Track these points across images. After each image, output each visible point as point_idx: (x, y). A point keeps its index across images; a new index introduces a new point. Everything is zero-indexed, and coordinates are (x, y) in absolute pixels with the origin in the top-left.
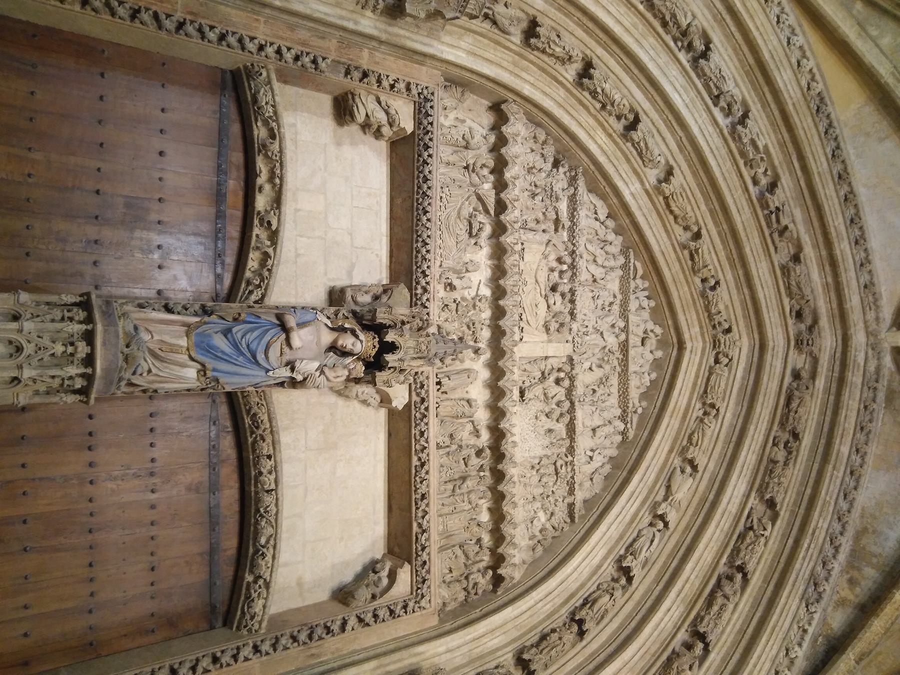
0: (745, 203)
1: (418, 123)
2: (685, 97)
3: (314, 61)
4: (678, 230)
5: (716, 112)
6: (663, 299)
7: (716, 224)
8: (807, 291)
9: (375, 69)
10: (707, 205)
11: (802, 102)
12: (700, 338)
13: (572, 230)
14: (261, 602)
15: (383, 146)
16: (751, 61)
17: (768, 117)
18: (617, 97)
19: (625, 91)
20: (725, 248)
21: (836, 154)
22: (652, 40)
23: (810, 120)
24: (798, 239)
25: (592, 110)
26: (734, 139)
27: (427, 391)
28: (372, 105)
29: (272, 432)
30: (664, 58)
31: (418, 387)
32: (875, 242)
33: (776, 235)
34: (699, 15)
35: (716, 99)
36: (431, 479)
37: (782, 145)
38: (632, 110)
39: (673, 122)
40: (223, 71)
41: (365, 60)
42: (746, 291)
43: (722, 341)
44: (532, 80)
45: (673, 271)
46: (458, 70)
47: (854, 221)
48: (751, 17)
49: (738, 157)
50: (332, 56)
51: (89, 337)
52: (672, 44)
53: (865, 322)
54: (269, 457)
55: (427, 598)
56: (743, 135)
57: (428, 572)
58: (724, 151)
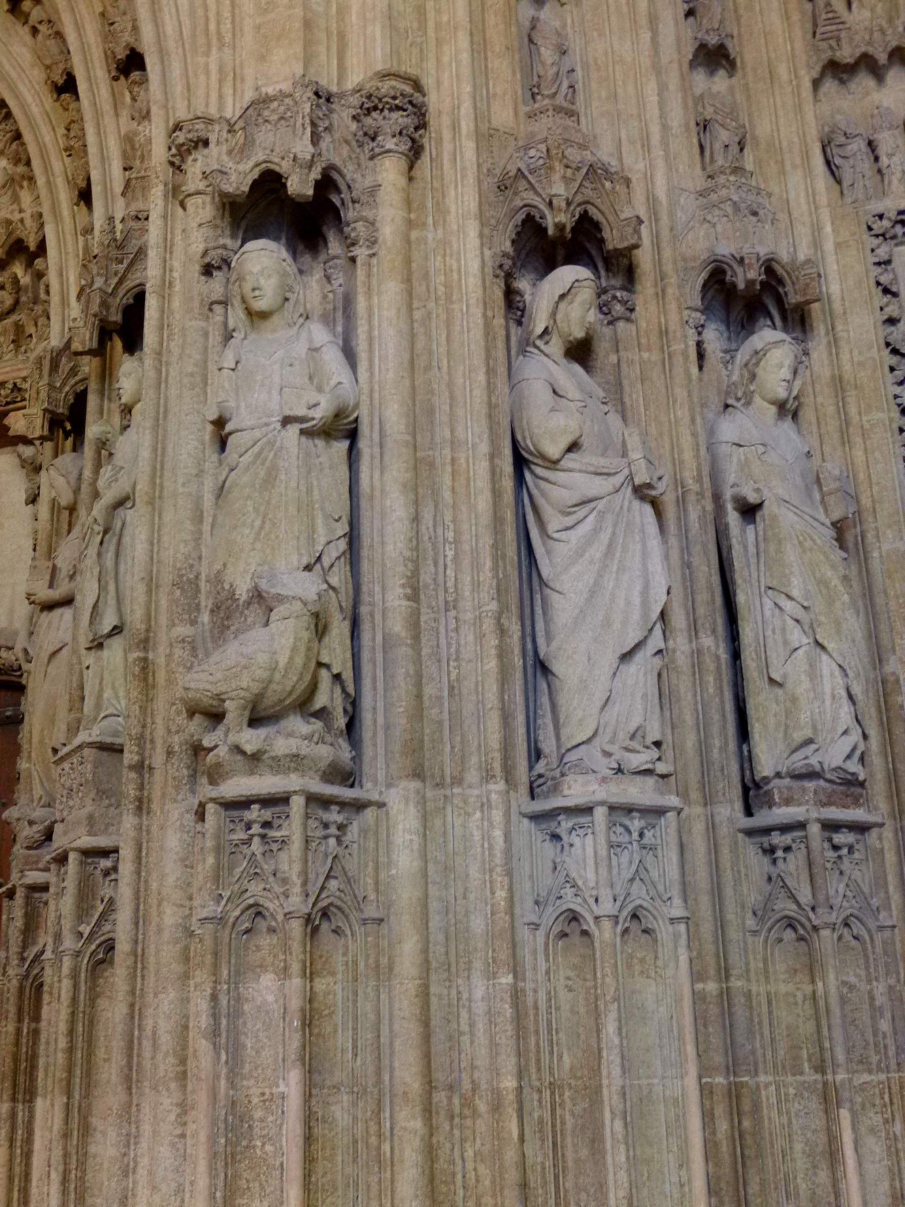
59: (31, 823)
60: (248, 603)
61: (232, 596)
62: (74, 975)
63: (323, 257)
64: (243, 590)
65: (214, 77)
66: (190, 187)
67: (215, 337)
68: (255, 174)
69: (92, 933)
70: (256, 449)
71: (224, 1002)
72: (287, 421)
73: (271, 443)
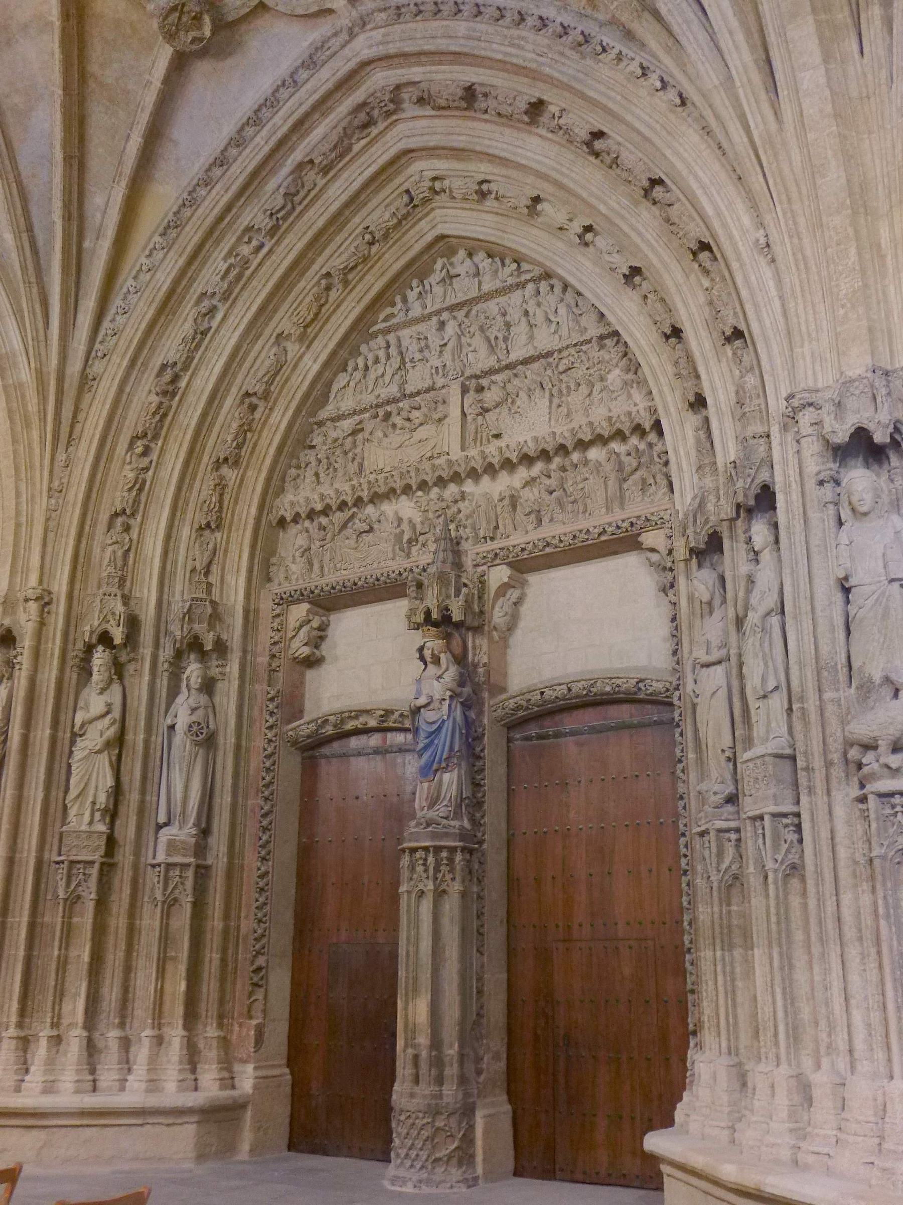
0: (283, 245)
1: (298, 601)
2: (213, 361)
3: (272, 700)
4: (333, 294)
5: (215, 323)
6: (405, 276)
7: (313, 262)
8: (334, 138)
9: (267, 650)
10: (299, 281)
11: (176, 246)
12: (431, 216)
13: (362, 411)
14: (654, 684)
15: (333, 617)
16: (163, 319)
17: (200, 271)
18: (235, 425)
19: (229, 416)
20: (332, 240)
21: (207, 182)
22: (181, 416)
23: (187, 229)
24: (292, 172)
25: (256, 437)
26: (230, 295)
27: (488, 552)
28: (296, 643)
29: (523, 694)
30: (191, 398)
31: (494, 558)
32: (264, 84)
33: (297, 199)
34: (147, 388)
35: (204, 333)
36: (558, 532)
37: (218, 242)
38: (242, 402)
39: (237, 360)
40: (303, 758)
41: (263, 660)
42: (363, 197)
43: (421, 196)
44: (246, 508)
45: (372, 281)
46: (254, 578)
47: (255, 120)
48: (131, 341)
49: (244, 279)
50: (266, 687)
51: (413, 850)
52: (177, 398)
53: (343, 47)
54: (542, 693)
55: (662, 514)
56: (222, 291)
57: (638, 517)
58: (246, 294)
59: (715, 793)
60: (881, 685)
61: (870, 680)
62: (776, 882)
63: (886, 466)
64: (877, 677)
65: (808, 359)
66: (804, 432)
67: (833, 522)
68: (852, 430)
69: (783, 860)
70: (875, 596)
71: (890, 900)
72: (892, 581)
73: (883, 593)
